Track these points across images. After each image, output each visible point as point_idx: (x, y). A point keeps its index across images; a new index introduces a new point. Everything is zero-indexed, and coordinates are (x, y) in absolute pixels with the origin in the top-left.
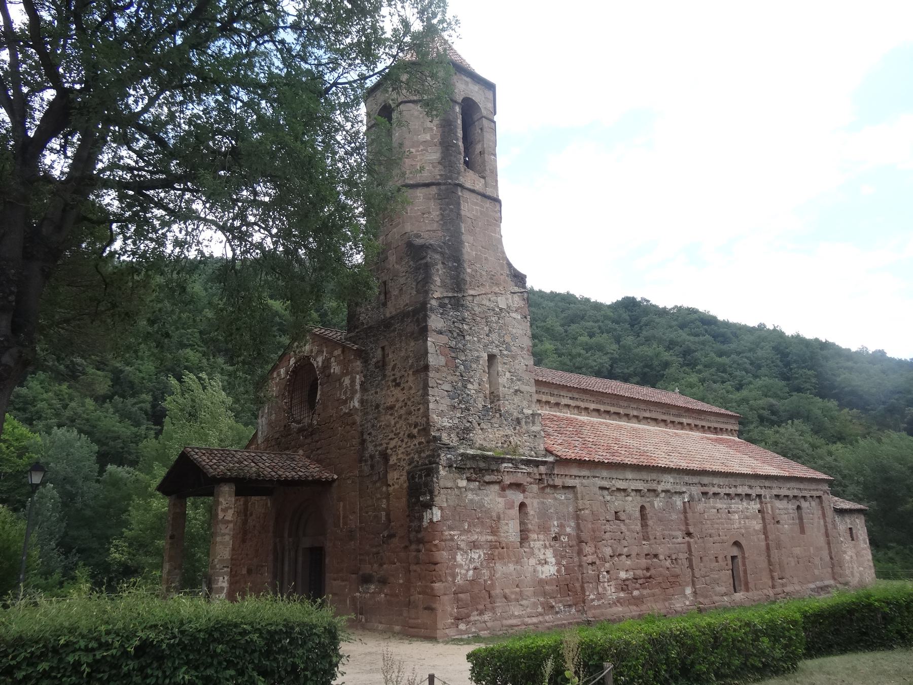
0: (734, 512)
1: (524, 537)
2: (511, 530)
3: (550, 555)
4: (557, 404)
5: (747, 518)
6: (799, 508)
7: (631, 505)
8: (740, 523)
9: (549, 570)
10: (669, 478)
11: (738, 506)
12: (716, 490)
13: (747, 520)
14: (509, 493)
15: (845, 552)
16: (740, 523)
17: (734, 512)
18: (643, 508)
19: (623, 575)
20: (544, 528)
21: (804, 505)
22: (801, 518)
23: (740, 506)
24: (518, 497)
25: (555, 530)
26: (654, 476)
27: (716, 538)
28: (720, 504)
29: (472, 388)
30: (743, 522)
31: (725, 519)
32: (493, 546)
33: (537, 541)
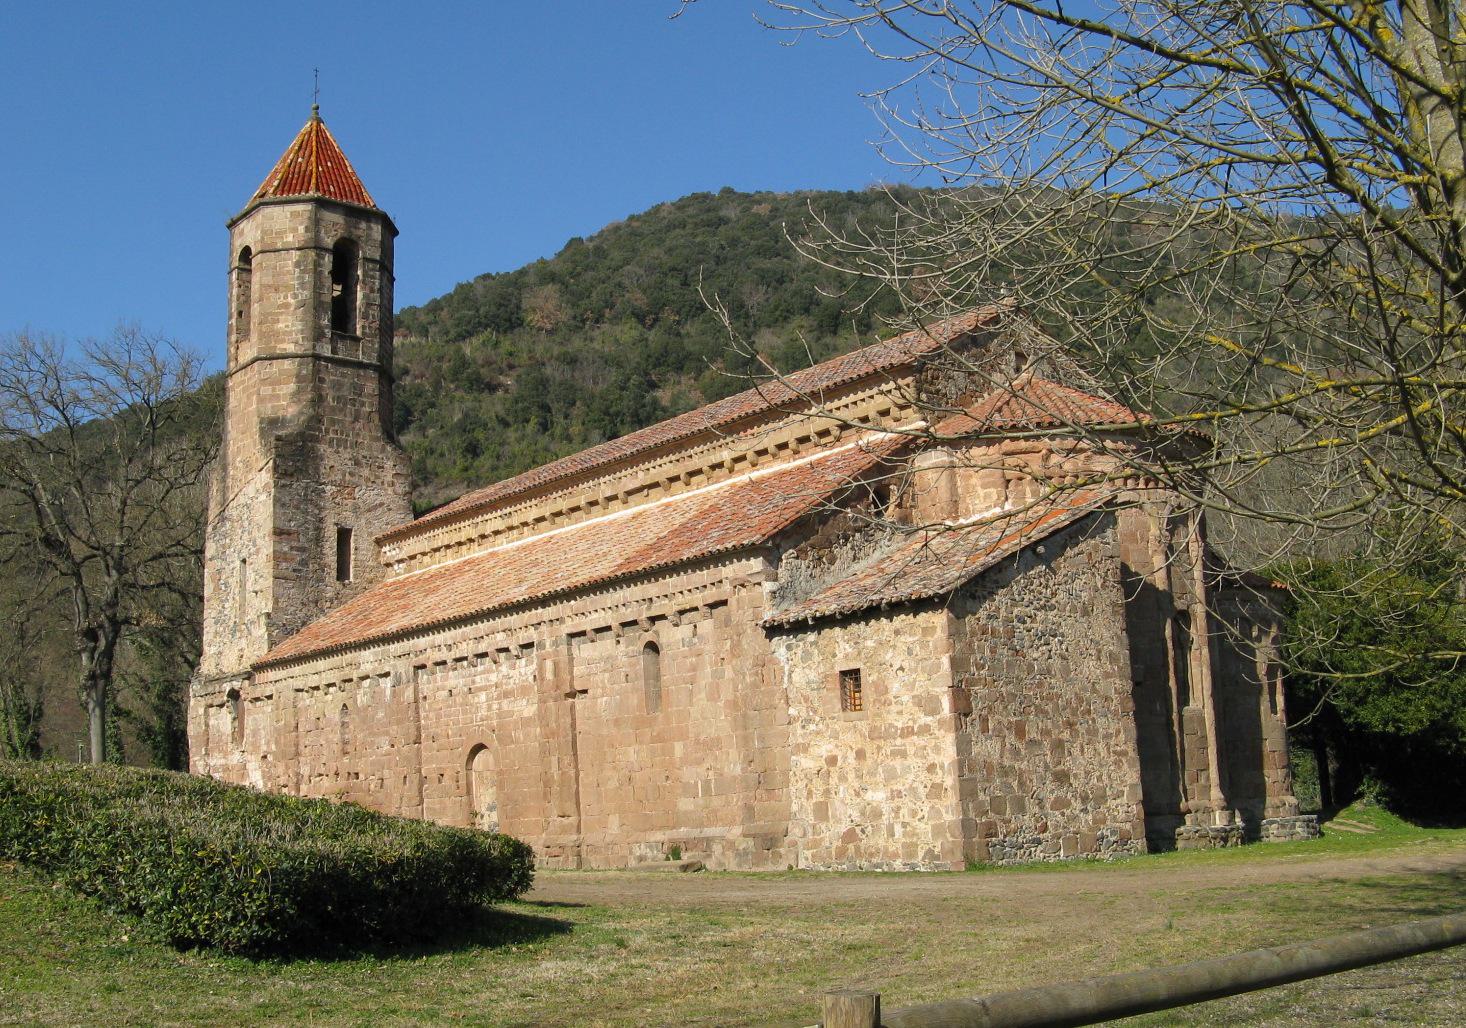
0: (480, 689)
5: (506, 695)
6: (653, 647)
8: (489, 708)
11: (488, 675)
12: (438, 656)
13: (505, 705)
15: (804, 748)
16: (489, 708)
17: (480, 689)
21: (666, 634)
22: (654, 676)
26: (349, 657)
27: (443, 741)
28: (455, 679)
30: (495, 707)
31: (461, 705)
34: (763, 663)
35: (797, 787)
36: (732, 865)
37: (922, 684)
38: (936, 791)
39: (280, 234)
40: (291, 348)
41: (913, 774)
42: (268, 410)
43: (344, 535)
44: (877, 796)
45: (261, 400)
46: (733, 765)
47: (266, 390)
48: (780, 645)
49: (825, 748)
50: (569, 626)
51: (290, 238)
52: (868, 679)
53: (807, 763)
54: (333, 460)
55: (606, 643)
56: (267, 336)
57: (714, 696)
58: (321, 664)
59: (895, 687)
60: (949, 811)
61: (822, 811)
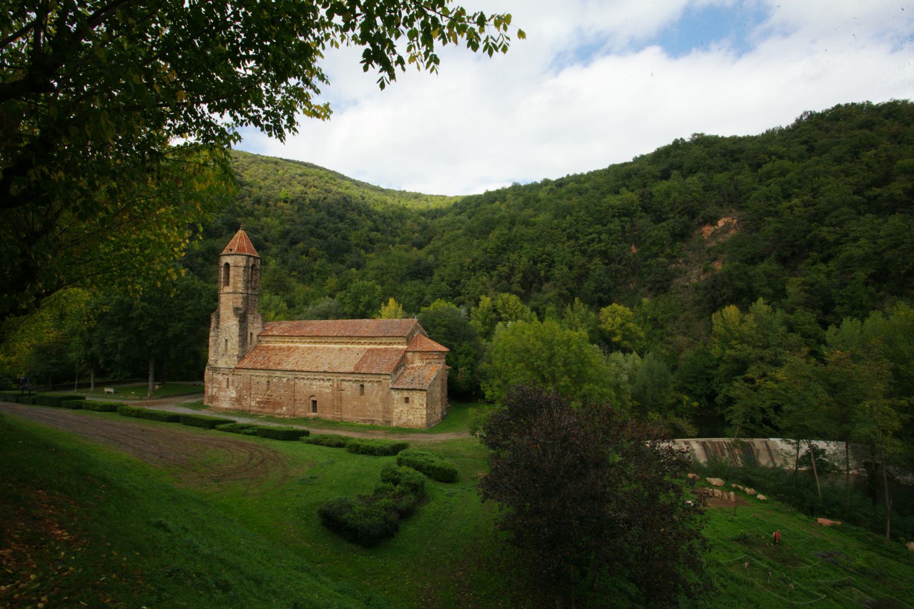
1: (228, 387)
2: (224, 385)
3: (234, 392)
4: (292, 342)
7: (264, 380)
9: (234, 395)
10: (279, 372)
14: (224, 376)
18: (268, 382)
19: (258, 400)
20: (233, 385)
21: (366, 384)
23: (318, 383)
24: (227, 377)
25: (236, 385)
29: (220, 350)
32: (219, 388)
33: (231, 388)
34: (388, 393)
35: (394, 414)
36: (379, 425)
37: (421, 402)
38: (422, 418)
39: (239, 263)
40: (241, 291)
41: (418, 415)
42: (235, 305)
43: (251, 334)
44: (411, 417)
45: (233, 303)
46: (380, 408)
47: (235, 300)
48: (393, 392)
49: (401, 409)
50: (341, 378)
51: (241, 264)
52: (410, 399)
53: (397, 410)
54: (250, 318)
55: (351, 383)
56: (235, 287)
57: (376, 396)
58: (261, 371)
59: (415, 401)
60: (424, 421)
61: (399, 418)
